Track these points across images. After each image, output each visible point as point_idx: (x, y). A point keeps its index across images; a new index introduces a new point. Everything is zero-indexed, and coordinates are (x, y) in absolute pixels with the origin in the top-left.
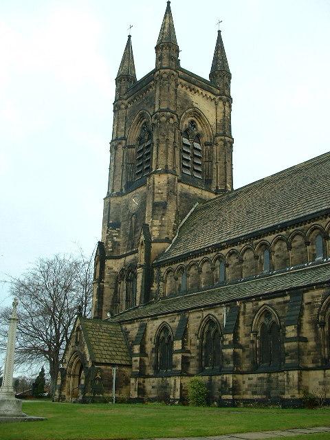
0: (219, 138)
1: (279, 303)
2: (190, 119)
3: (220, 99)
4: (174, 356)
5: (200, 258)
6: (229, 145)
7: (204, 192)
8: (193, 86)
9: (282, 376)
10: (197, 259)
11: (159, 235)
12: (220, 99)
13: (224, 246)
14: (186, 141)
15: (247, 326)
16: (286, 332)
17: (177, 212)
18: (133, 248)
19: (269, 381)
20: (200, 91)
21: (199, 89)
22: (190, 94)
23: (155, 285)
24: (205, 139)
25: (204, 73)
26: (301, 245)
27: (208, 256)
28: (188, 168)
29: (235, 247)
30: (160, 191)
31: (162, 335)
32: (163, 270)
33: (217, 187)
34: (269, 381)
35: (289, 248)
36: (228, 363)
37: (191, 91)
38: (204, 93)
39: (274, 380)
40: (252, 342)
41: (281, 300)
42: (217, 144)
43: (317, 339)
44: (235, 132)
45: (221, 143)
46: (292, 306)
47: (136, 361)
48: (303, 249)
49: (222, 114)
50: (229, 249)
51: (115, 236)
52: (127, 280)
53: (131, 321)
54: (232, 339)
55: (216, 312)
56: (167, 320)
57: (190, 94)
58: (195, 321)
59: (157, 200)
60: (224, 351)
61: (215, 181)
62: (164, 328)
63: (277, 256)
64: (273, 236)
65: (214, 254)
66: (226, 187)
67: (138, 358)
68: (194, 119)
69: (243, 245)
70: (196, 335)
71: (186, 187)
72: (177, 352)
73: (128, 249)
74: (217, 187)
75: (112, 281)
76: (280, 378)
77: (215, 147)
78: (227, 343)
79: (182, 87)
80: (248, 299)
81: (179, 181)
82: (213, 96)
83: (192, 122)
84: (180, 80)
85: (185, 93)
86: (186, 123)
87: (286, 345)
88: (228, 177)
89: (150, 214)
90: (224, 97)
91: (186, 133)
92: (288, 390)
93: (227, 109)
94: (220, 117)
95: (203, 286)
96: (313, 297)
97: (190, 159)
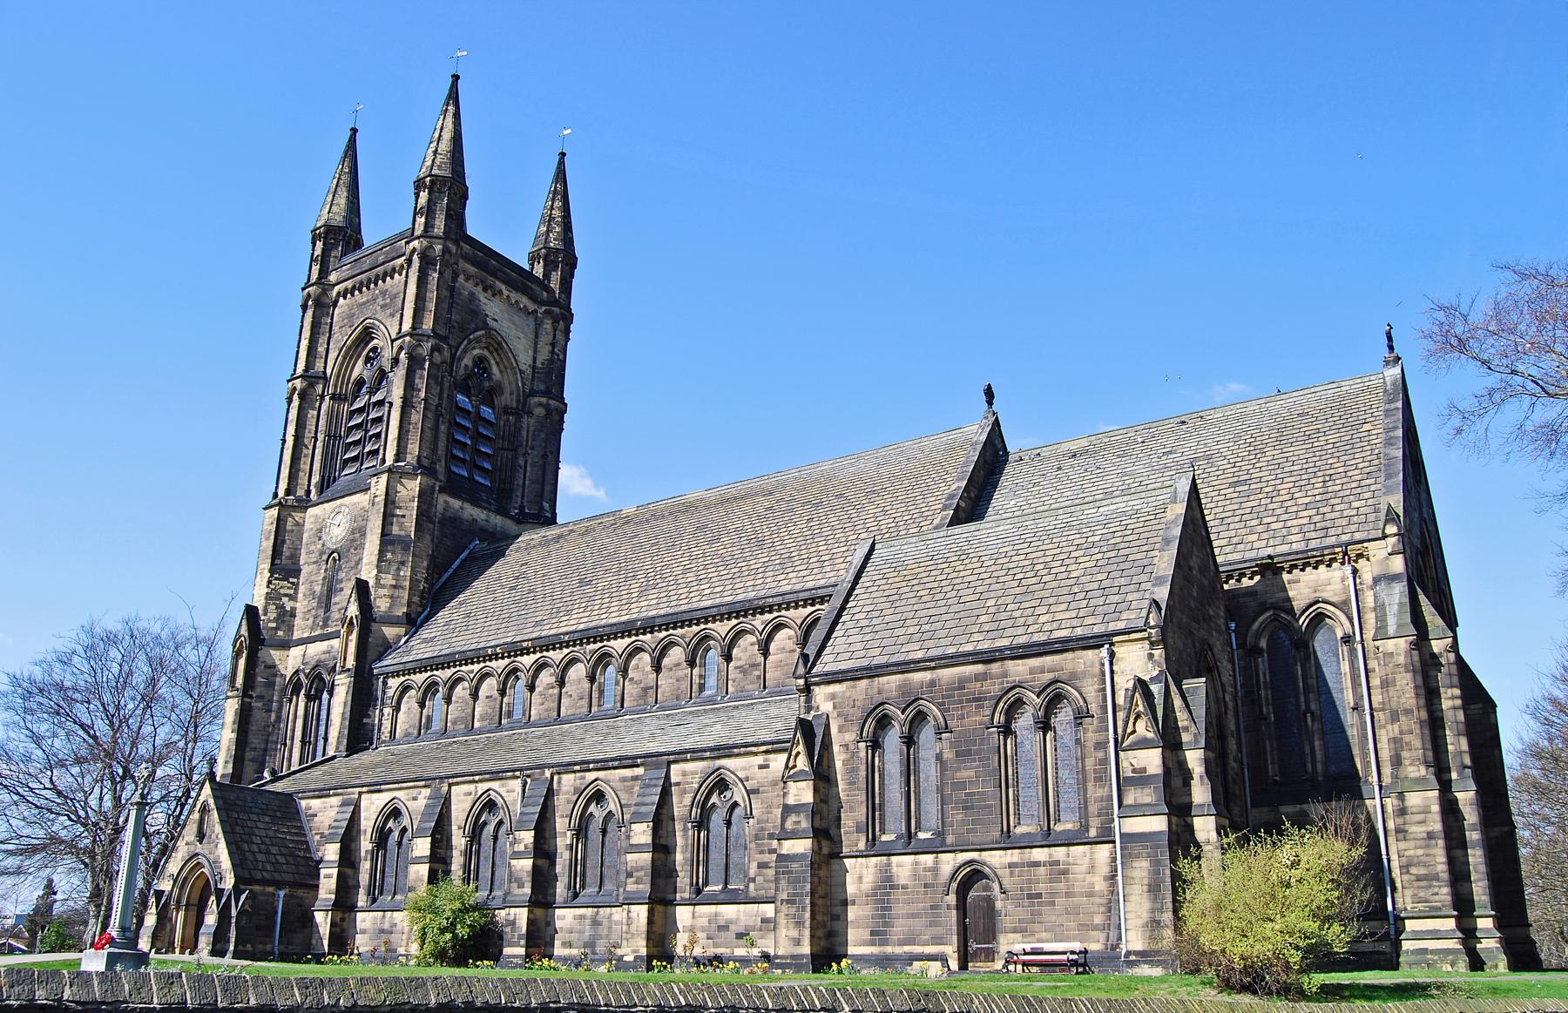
0: (537, 399)
1: (624, 780)
2: (476, 352)
5: (476, 667)
6: (557, 418)
7: (492, 516)
8: (490, 280)
9: (618, 914)
10: (470, 667)
11: (390, 608)
13: (527, 649)
16: (632, 834)
17: (432, 558)
19: (595, 923)
20: (506, 293)
21: (503, 287)
22: (482, 297)
24: (507, 399)
25: (518, 249)
26: (679, 664)
27: (493, 664)
28: (464, 461)
31: (391, 824)
32: (394, 683)
33: (522, 508)
34: (595, 923)
35: (657, 667)
36: (521, 886)
37: (485, 290)
38: (515, 296)
39: (605, 923)
41: (627, 772)
42: (530, 413)
44: (572, 391)
45: (539, 411)
46: (648, 786)
47: (328, 876)
48: (681, 673)
49: (549, 348)
50: (538, 655)
52: (309, 697)
53: (322, 793)
54: (532, 840)
55: (503, 786)
57: (482, 299)
58: (460, 801)
60: (513, 862)
61: (519, 493)
62: (395, 813)
64: (627, 641)
65: (507, 661)
66: (542, 508)
67: (335, 872)
68: (486, 353)
69: (566, 651)
71: (456, 503)
72: (418, 861)
74: (522, 508)
76: (616, 917)
77: (525, 420)
78: (521, 848)
79: (468, 279)
80: (567, 768)
81: (441, 490)
82: (531, 306)
83: (480, 361)
84: (464, 265)
85: (472, 294)
86: (467, 361)
87: (629, 857)
88: (548, 488)
89: (375, 559)
90: (556, 310)
92: (627, 940)
93: (560, 337)
94: (544, 354)
95: (477, 724)
96: (684, 774)
97: (469, 443)
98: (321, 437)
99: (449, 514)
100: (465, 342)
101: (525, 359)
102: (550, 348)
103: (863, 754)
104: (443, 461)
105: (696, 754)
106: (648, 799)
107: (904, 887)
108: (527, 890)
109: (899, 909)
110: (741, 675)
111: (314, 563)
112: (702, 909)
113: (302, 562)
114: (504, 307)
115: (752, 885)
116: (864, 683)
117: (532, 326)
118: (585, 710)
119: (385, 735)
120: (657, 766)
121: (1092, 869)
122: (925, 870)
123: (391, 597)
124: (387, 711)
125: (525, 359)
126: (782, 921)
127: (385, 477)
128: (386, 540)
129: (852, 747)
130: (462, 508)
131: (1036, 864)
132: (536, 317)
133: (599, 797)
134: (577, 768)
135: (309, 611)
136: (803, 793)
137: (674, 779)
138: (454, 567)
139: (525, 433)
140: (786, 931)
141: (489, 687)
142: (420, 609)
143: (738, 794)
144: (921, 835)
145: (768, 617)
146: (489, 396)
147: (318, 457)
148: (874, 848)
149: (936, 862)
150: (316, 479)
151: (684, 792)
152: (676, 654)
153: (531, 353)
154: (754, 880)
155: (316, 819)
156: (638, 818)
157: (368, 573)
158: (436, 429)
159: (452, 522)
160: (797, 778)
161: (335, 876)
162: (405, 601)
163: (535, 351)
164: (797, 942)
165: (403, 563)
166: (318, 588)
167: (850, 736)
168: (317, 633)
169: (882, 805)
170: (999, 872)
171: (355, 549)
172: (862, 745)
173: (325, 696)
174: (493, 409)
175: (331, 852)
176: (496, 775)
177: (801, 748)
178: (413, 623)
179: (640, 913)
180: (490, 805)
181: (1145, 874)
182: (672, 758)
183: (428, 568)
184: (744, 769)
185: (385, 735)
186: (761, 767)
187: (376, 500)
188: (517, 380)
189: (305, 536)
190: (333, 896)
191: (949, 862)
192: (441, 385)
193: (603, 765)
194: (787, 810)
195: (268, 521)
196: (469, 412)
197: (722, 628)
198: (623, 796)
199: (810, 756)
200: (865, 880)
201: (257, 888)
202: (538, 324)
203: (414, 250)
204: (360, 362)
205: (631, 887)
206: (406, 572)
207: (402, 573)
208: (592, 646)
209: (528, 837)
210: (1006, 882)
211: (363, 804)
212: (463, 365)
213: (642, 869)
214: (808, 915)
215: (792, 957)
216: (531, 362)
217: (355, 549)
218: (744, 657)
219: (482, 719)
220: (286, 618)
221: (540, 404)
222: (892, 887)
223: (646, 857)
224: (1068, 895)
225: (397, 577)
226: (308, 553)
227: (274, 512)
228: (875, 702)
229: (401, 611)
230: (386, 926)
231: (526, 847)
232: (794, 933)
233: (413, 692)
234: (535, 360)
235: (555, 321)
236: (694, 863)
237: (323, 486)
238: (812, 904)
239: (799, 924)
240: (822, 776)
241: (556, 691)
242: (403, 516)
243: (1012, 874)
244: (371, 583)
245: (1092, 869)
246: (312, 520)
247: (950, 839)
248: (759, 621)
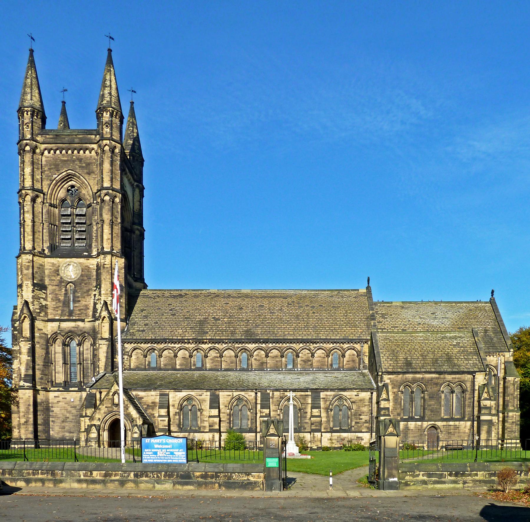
10: (173, 345)
35: (267, 356)
40: (279, 415)
41: (303, 393)
43: (328, 417)
46: (315, 398)
51: (42, 298)
55: (246, 394)
63: (255, 359)
73: (61, 315)
95: (178, 367)
96: (326, 395)
107: (412, 430)
111: (56, 285)
121: (465, 427)
122: (418, 426)
131: (451, 425)
149: (422, 424)
154: (354, 427)
166: (62, 298)
168: (65, 318)
181: (486, 429)
198: (301, 400)
203: (106, 145)
210: (442, 429)
220: (43, 308)
224: (458, 433)
243: (444, 428)
245: (465, 427)
247: (426, 419)
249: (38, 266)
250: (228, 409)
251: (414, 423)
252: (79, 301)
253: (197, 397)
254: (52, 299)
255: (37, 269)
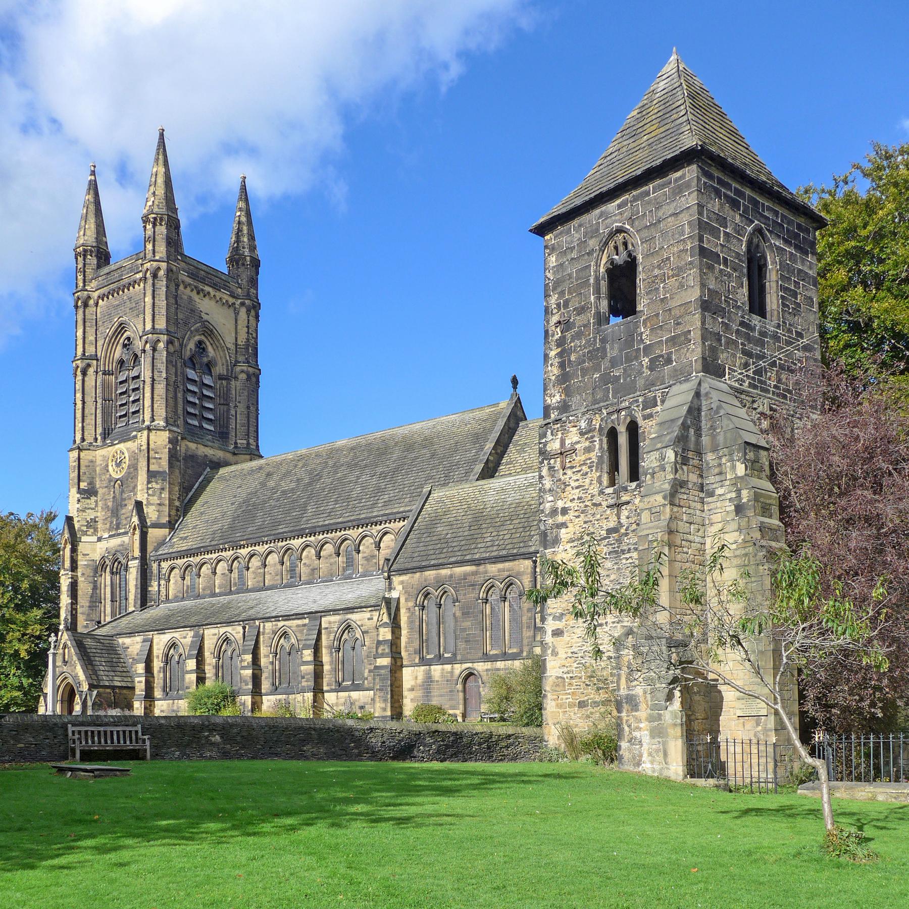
1: (298, 626)
2: (197, 338)
3: (242, 304)
4: (187, 676)
5: (214, 556)
6: (254, 379)
9: (299, 697)
10: (210, 556)
11: (158, 518)
12: (242, 304)
14: (191, 374)
15: (267, 646)
17: (181, 484)
18: (118, 528)
23: (155, 584)
26: (331, 555)
28: (195, 415)
29: (257, 548)
30: (157, 456)
31: (172, 651)
32: (165, 565)
35: (319, 557)
41: (299, 622)
42: (236, 378)
45: (243, 376)
47: (140, 682)
48: (332, 560)
50: (250, 549)
52: (112, 573)
54: (251, 660)
55: (233, 630)
56: (176, 635)
58: (210, 639)
59: (153, 468)
60: (242, 672)
62: (173, 645)
64: (301, 541)
65: (231, 552)
67: (143, 679)
68: (203, 338)
69: (266, 546)
70: (211, 653)
71: (193, 446)
72: (190, 672)
75: (89, 572)
78: (246, 664)
80: (267, 619)
82: (231, 300)
86: (191, 345)
87: (302, 668)
91: (192, 362)
95: (217, 591)
96: (330, 623)
97: (197, 402)
98: (99, 401)
99: (189, 453)
100: (189, 333)
101: (229, 340)
102: (246, 329)
103: (417, 613)
104: (182, 417)
105: (335, 611)
106: (310, 637)
107: (437, 681)
108: (250, 686)
109: (435, 693)
110: (366, 562)
111: (106, 487)
112: (341, 694)
113: (98, 486)
114: (213, 303)
115: (366, 681)
116: (418, 574)
117: (233, 315)
118: (279, 582)
119: (163, 598)
120: (315, 619)
122: (447, 673)
123: (158, 511)
124: (162, 582)
125: (229, 340)
126: (377, 699)
127: (145, 432)
128: (152, 475)
129: (412, 609)
130: (197, 448)
132: (235, 309)
133: (285, 635)
134: (273, 620)
135: (106, 518)
136: (386, 634)
137: (323, 626)
138: (195, 487)
139: (234, 392)
140: (379, 705)
141: (222, 567)
142: (177, 518)
143: (358, 634)
144: (446, 655)
145: (379, 527)
146: (208, 367)
147: (99, 416)
148: (424, 662)
149: (453, 669)
150: (99, 430)
151: (330, 633)
152: (329, 549)
153: (234, 335)
154: (367, 679)
155: (129, 650)
156: (306, 647)
157: (141, 496)
158: (175, 397)
159: (191, 458)
160: (385, 625)
161: (144, 682)
162: (167, 514)
163: (236, 333)
164: (384, 710)
165: (163, 489)
166: (110, 504)
167: (411, 604)
169: (427, 640)
170: (481, 673)
171: (132, 479)
172: (417, 608)
173: (123, 573)
174: (212, 376)
175: (140, 668)
176: (229, 623)
177: (384, 610)
178: (171, 525)
179: (309, 696)
180: (227, 640)
182: (323, 614)
183: (180, 490)
184: (360, 620)
185: (163, 598)
186: (369, 619)
187: (142, 448)
188: (225, 354)
189: (98, 469)
190: (144, 693)
191: (458, 668)
192: (176, 366)
193: (287, 617)
194: (379, 643)
195: (72, 459)
196: (195, 381)
197: (354, 533)
198: (298, 635)
199: (389, 614)
200: (419, 678)
201: (101, 690)
202: (237, 314)
204: (119, 347)
205: (304, 684)
206: (166, 495)
207: (163, 496)
208: (280, 544)
209: (248, 658)
211: (155, 641)
212: (188, 348)
213: (309, 674)
214: (389, 696)
215: (383, 717)
216: (234, 341)
217: (132, 479)
218: (368, 551)
219: (220, 587)
221: (242, 371)
222: (431, 682)
223: (311, 668)
225: (160, 498)
226: (101, 480)
227: (75, 454)
228: (424, 584)
229: (165, 520)
230: (175, 708)
231: (248, 663)
232: (383, 705)
233: (176, 571)
234: (236, 341)
235: (248, 311)
236: (335, 670)
237: (106, 434)
238: (392, 691)
239: (385, 701)
240: (395, 626)
241: (262, 571)
242: (160, 458)
244: (145, 502)
246: (101, 458)
247: (459, 657)
248: (375, 530)
249: (87, 464)
250: (214, 658)
251: (439, 667)
252: (126, 505)
253: (181, 640)
254: (102, 508)
255: (85, 468)
